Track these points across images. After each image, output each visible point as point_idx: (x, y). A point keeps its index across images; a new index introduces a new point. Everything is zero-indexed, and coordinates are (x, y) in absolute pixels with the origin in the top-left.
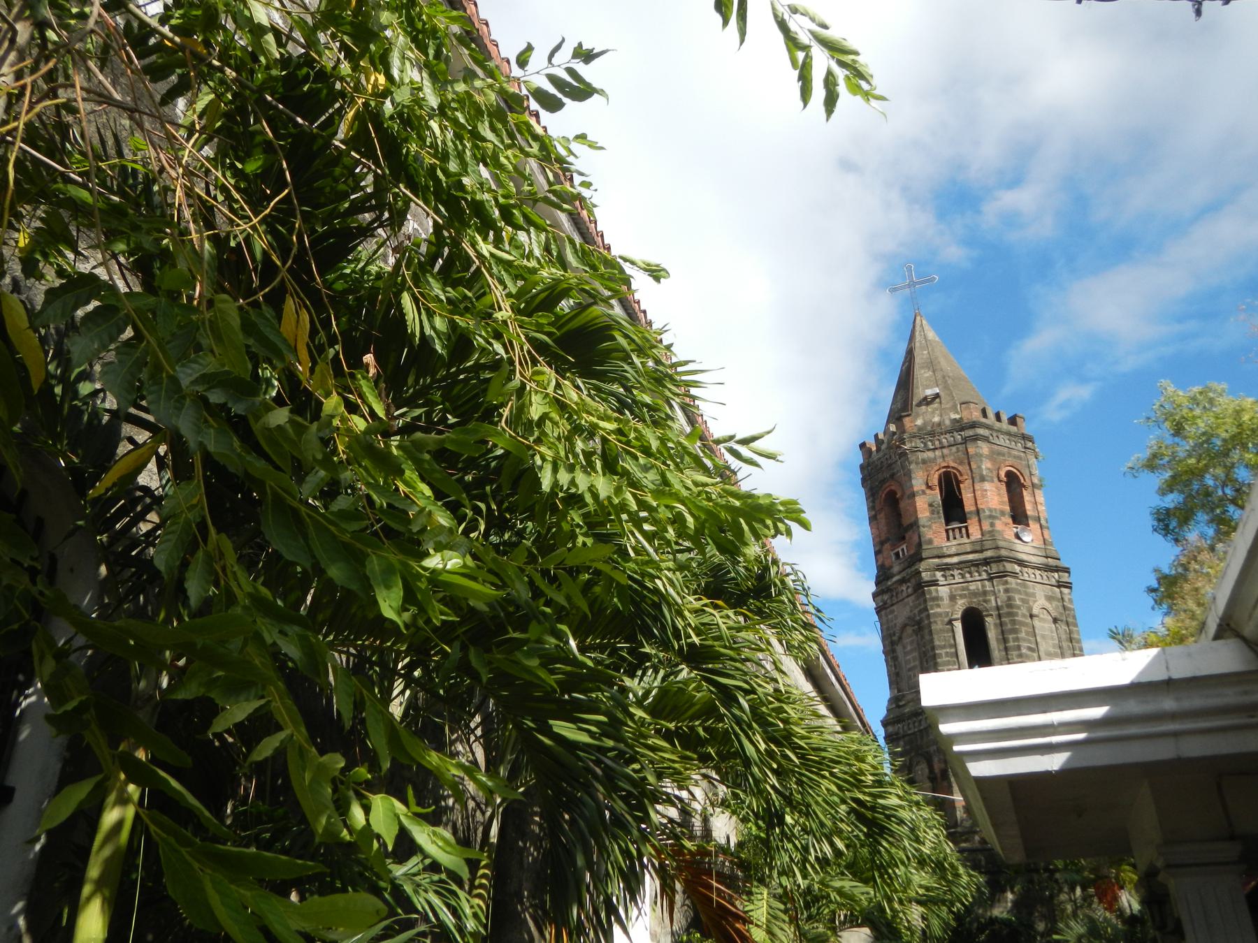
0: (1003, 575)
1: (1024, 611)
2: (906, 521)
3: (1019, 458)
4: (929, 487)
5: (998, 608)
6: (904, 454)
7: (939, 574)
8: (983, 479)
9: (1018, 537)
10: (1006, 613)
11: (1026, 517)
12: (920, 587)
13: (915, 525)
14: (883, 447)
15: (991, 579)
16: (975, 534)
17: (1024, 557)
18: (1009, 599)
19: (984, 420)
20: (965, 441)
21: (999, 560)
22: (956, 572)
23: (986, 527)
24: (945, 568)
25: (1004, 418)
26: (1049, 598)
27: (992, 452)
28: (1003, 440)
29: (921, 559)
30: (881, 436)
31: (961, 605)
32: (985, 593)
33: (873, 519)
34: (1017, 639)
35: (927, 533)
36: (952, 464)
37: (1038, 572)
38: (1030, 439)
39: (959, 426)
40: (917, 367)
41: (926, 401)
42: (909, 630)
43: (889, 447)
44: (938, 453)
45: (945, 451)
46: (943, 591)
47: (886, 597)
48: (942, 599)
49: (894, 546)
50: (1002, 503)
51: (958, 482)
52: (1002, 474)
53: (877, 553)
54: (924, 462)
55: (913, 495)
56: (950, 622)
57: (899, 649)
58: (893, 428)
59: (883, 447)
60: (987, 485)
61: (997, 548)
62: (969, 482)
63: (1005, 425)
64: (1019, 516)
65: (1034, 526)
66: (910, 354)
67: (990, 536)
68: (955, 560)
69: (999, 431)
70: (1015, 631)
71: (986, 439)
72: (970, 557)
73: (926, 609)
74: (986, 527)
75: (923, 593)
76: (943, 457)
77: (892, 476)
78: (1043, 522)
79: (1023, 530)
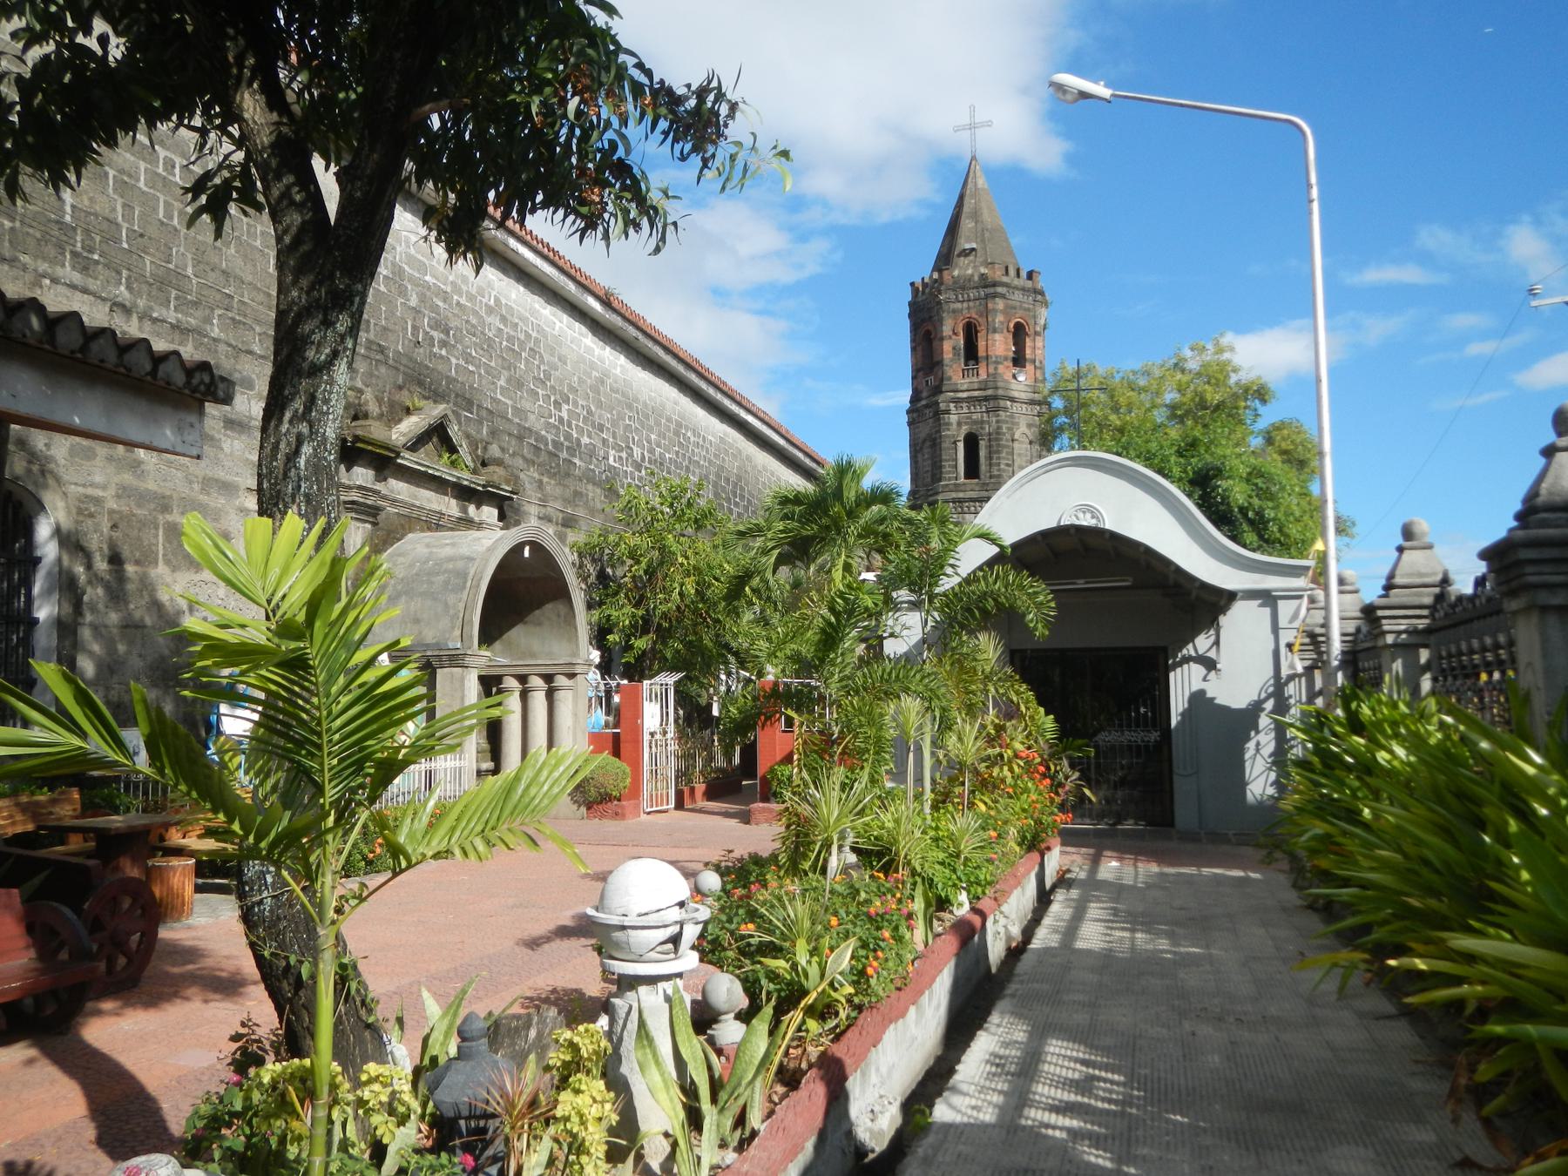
0: (997, 409)
1: (1008, 436)
2: (936, 359)
3: (1029, 310)
4: (955, 334)
5: (990, 434)
6: (939, 303)
7: (952, 405)
8: (995, 331)
9: (1014, 377)
10: (995, 437)
11: (1025, 360)
12: (938, 414)
13: (940, 363)
14: (927, 291)
15: (988, 412)
16: (983, 376)
17: (1016, 394)
18: (999, 428)
19: (1005, 279)
20: (987, 296)
21: (995, 398)
22: (964, 405)
23: (991, 370)
24: (957, 401)
25: (1024, 274)
26: (1029, 426)
27: (1007, 306)
28: (1018, 296)
29: (941, 392)
30: (926, 280)
31: (965, 429)
32: (982, 422)
33: (914, 349)
34: (999, 458)
35: (949, 372)
36: (974, 316)
37: (1024, 406)
38: (1042, 293)
39: (985, 282)
40: (963, 216)
41: (966, 253)
42: (928, 444)
43: (931, 293)
44: (965, 305)
45: (971, 304)
46: (953, 418)
47: (915, 415)
48: (951, 424)
49: (927, 375)
50: (1008, 350)
51: (977, 332)
52: (1012, 325)
53: (914, 378)
54: (954, 311)
55: (942, 339)
56: (955, 443)
57: (919, 455)
58: (936, 276)
59: (927, 291)
60: (997, 336)
61: (996, 388)
62: (984, 332)
63: (1023, 281)
64: (1019, 360)
65: (1029, 367)
66: (961, 198)
67: (994, 377)
68: (965, 395)
69: (1016, 288)
70: (998, 452)
71: (1003, 296)
72: (976, 393)
73: (939, 431)
74: (991, 370)
75: (939, 419)
76: (969, 308)
77: (931, 317)
78: (1037, 364)
79: (1020, 372)
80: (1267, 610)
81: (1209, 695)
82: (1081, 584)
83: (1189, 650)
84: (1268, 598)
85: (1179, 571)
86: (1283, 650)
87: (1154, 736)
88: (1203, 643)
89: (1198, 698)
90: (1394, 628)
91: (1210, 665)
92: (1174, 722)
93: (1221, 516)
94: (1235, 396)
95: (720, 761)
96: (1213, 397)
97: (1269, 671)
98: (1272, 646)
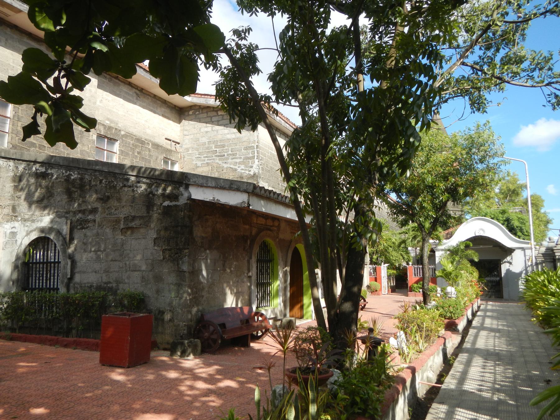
80: (523, 252)
81: (511, 269)
82: (481, 247)
83: (505, 260)
84: (523, 249)
85: (503, 245)
86: (527, 260)
87: (498, 279)
88: (509, 258)
89: (508, 271)
90: (539, 260)
91: (510, 263)
92: (502, 276)
93: (512, 230)
94: (518, 188)
95: (392, 284)
96: (512, 187)
97: (524, 265)
98: (524, 259)
